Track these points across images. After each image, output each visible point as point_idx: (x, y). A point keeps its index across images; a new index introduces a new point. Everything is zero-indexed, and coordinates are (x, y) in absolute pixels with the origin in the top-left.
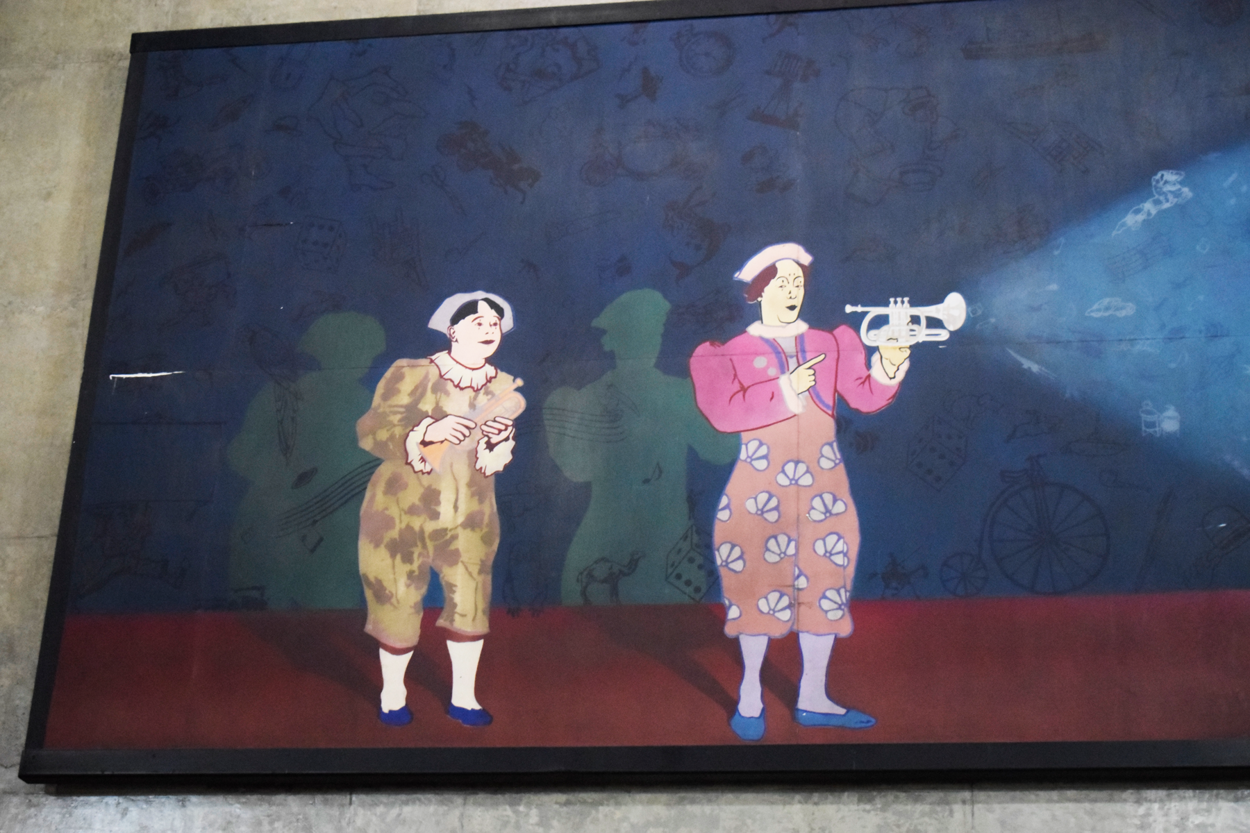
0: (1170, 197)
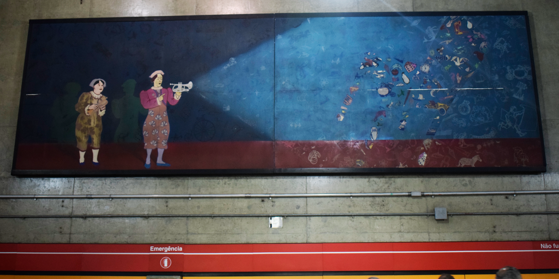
0: (232, 63)
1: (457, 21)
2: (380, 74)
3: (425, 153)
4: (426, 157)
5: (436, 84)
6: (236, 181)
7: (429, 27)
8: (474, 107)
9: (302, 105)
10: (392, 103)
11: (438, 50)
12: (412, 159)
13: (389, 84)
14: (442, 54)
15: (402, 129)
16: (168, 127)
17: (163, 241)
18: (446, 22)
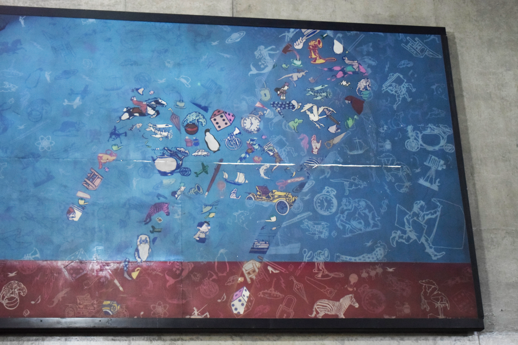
3: (245, 288)
4: (247, 297)
5: (272, 154)
7: (262, 47)
8: (344, 200)
10: (183, 188)
11: (277, 90)
12: (219, 301)
13: (178, 150)
14: (284, 98)
15: (202, 241)
18: (295, 39)
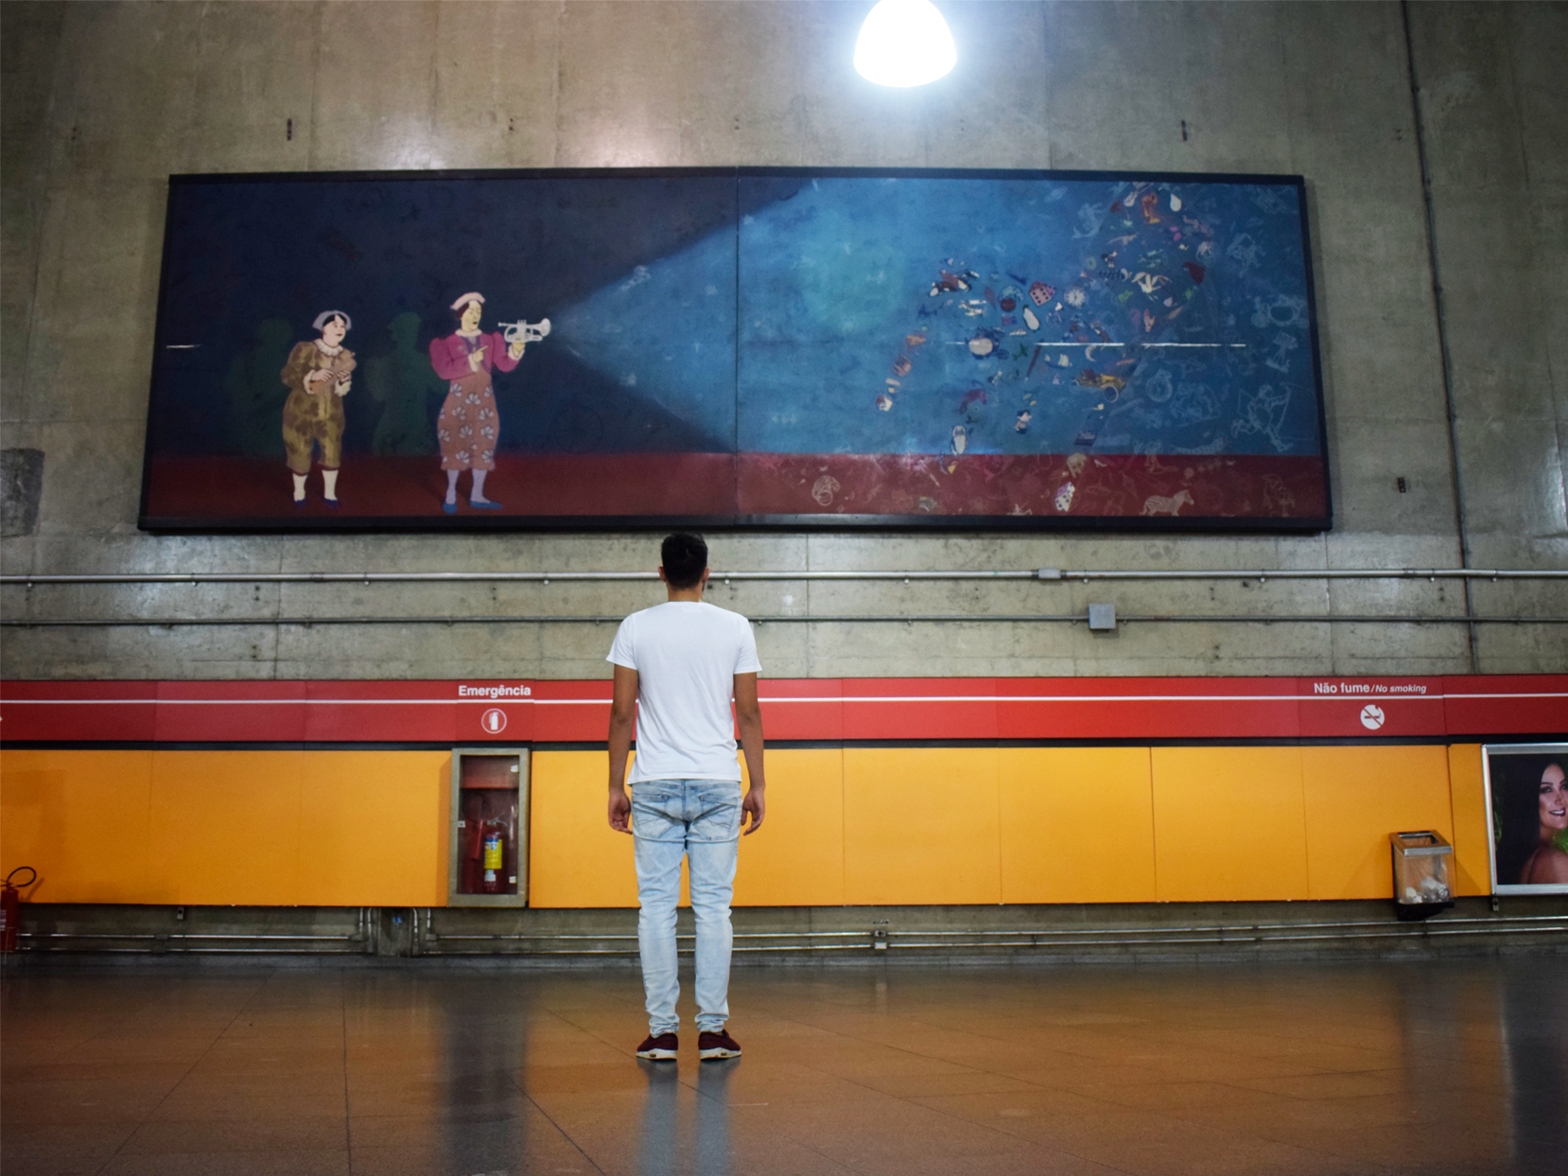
1: (1147, 192)
2: (975, 307)
5: (1098, 332)
6: (649, 542)
7: (1087, 206)
8: (1180, 386)
9: (798, 374)
11: (1104, 256)
15: (1022, 431)
16: (496, 422)
17: (487, 676)
